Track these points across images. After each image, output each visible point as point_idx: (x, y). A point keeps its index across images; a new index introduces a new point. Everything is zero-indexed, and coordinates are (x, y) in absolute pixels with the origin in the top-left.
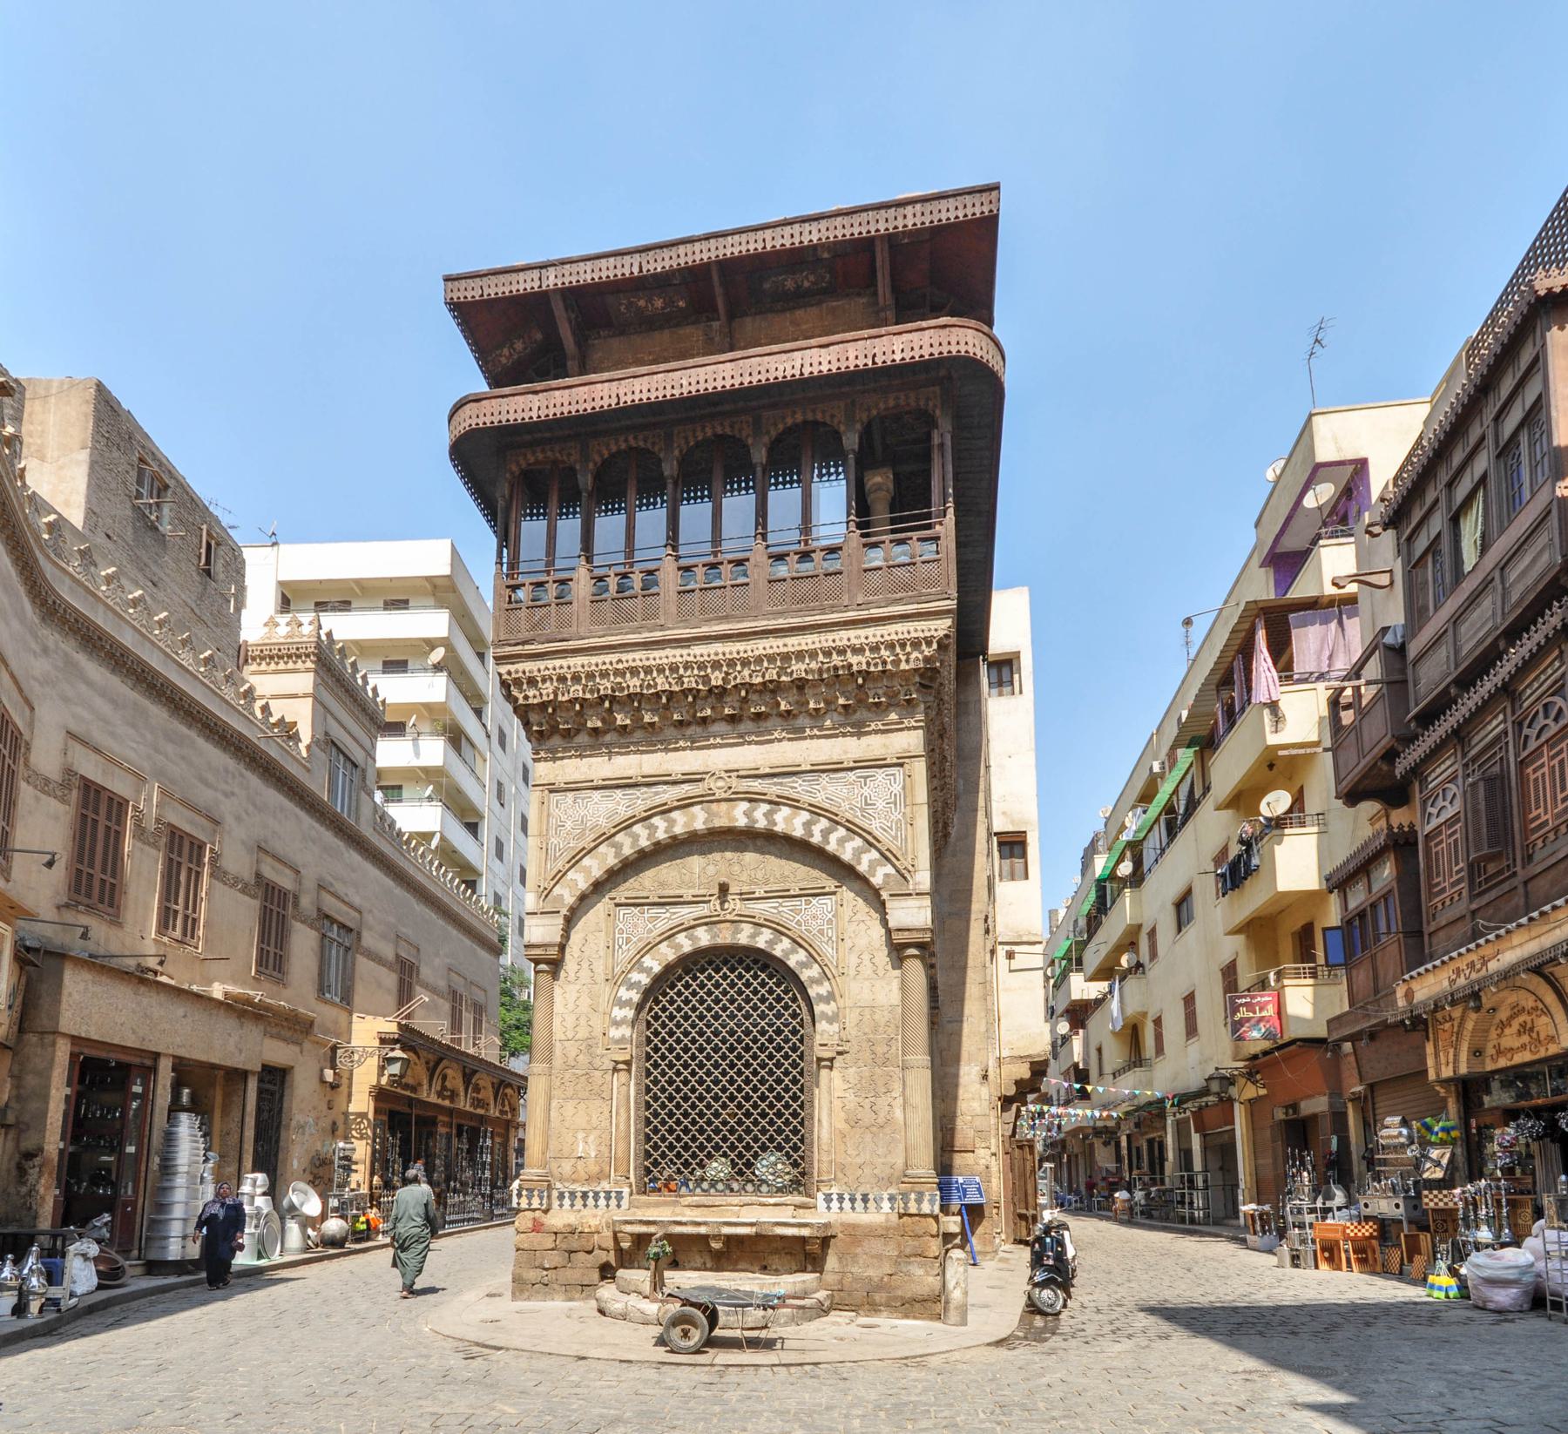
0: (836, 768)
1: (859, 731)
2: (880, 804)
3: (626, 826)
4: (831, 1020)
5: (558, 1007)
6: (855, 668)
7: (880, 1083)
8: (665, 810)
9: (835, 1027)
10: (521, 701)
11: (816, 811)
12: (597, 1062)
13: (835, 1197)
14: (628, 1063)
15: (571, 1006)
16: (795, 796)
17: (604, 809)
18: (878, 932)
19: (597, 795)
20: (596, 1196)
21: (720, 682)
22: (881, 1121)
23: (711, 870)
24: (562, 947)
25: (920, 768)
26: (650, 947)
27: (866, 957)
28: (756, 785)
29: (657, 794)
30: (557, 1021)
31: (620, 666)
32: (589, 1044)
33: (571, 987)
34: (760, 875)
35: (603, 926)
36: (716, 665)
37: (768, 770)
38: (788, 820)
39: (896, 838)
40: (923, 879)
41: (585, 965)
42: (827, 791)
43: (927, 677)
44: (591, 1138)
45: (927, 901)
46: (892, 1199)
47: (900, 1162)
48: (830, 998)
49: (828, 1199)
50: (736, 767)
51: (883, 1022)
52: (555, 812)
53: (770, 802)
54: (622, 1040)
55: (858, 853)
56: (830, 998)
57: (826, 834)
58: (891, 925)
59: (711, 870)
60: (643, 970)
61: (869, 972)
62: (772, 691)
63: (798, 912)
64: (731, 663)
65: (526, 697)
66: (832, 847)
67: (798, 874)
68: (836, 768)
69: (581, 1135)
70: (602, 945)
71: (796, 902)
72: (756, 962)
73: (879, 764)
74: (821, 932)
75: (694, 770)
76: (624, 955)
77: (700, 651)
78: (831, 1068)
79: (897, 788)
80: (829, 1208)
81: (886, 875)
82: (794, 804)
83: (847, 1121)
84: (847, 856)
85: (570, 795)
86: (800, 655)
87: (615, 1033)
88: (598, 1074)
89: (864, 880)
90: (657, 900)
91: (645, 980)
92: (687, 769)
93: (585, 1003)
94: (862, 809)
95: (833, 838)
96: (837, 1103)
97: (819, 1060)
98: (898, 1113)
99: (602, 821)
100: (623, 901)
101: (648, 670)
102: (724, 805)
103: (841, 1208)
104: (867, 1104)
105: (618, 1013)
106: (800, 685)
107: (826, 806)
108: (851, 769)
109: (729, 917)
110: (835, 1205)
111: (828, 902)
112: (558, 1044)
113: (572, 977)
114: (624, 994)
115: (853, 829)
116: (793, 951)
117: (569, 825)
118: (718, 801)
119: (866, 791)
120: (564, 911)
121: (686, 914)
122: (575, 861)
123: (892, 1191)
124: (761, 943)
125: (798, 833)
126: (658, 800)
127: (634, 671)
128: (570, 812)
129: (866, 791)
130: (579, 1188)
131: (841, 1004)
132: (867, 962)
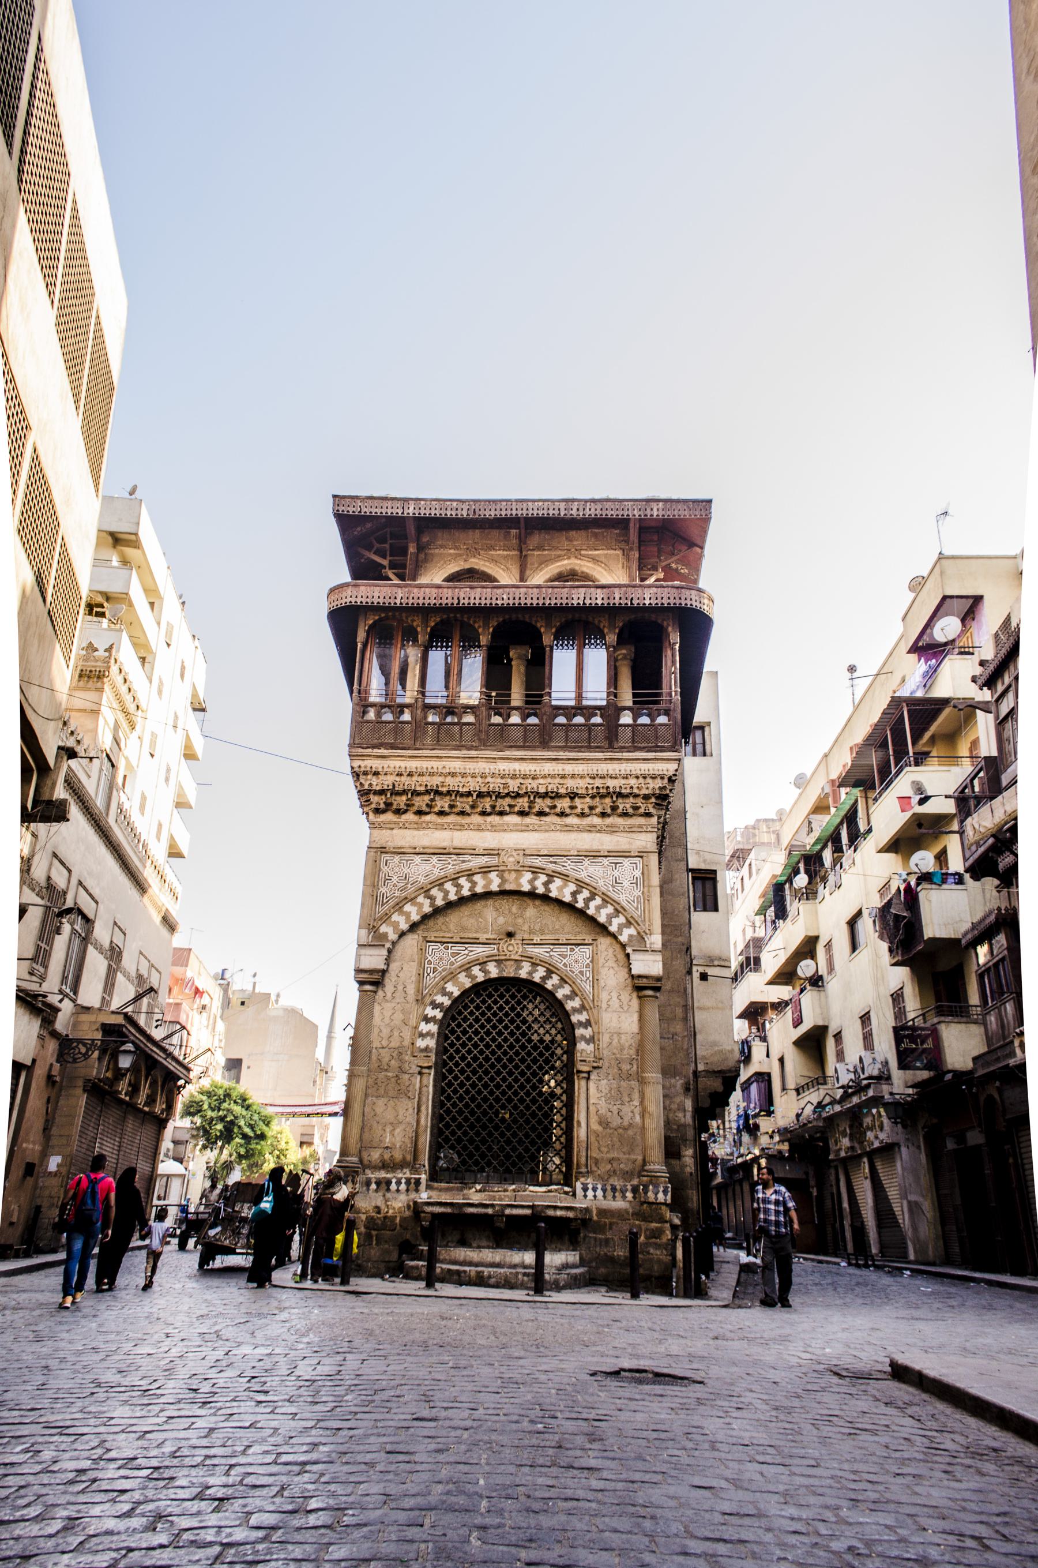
0: (594, 855)
1: (612, 830)
2: (626, 884)
3: (439, 883)
4: (591, 1040)
6: (611, 790)
7: (625, 1095)
8: (470, 875)
9: (590, 1048)
10: (366, 787)
11: (581, 885)
12: (406, 1066)
13: (590, 1186)
14: (429, 1068)
15: (387, 1020)
16: (566, 872)
17: (422, 870)
18: (623, 974)
19: (417, 859)
20: (399, 1183)
21: (516, 790)
22: (626, 1123)
23: (501, 920)
24: (384, 972)
25: (654, 859)
26: (452, 976)
27: (614, 995)
28: (538, 862)
29: (464, 862)
30: (376, 1031)
31: (444, 771)
33: (388, 1005)
34: (537, 927)
35: (416, 957)
36: (514, 777)
37: (546, 853)
38: (560, 889)
39: (637, 909)
40: (656, 940)
41: (400, 988)
42: (588, 871)
43: (662, 799)
44: (398, 1130)
45: (659, 957)
46: (635, 1190)
47: (640, 1158)
48: (587, 1024)
49: (585, 1189)
50: (523, 847)
51: (627, 1045)
52: (385, 869)
53: (547, 875)
54: (427, 1049)
55: (610, 917)
56: (587, 1024)
57: (587, 901)
58: (634, 972)
59: (501, 920)
60: (444, 993)
61: (617, 1006)
62: (552, 798)
63: (565, 957)
64: (525, 777)
65: (370, 785)
66: (591, 912)
67: (565, 925)
68: (594, 855)
69: (388, 1130)
70: (414, 972)
71: (563, 949)
72: (530, 991)
73: (625, 854)
74: (581, 972)
75: (492, 847)
76: (431, 980)
78: (588, 1079)
79: (638, 873)
80: (585, 1196)
81: (631, 936)
82: (565, 877)
83: (600, 1123)
84: (602, 919)
85: (397, 858)
86: (573, 776)
87: (421, 1043)
88: (407, 1076)
89: (614, 936)
90: (458, 940)
91: (447, 1002)
92: (487, 845)
93: (399, 1017)
94: (613, 886)
95: (592, 905)
96: (592, 1108)
97: (579, 1072)
98: (638, 1118)
99: (422, 880)
100: (433, 939)
101: (464, 775)
102: (513, 875)
103: (595, 1196)
104: (615, 1109)
105: (424, 1027)
106: (573, 796)
107: (587, 881)
108: (606, 856)
109: (512, 957)
110: (590, 1193)
111: (587, 951)
112: (374, 1050)
113: (389, 994)
114: (430, 1012)
115: (606, 900)
116: (561, 986)
117: (395, 879)
118: (510, 871)
119: (616, 873)
120: (388, 945)
121: (480, 951)
122: (399, 907)
123: (635, 1182)
124: (537, 978)
125: (567, 899)
126: (465, 866)
127: (453, 775)
128: (397, 869)
129: (616, 873)
130: (383, 1174)
131: (596, 1030)
132: (615, 998)
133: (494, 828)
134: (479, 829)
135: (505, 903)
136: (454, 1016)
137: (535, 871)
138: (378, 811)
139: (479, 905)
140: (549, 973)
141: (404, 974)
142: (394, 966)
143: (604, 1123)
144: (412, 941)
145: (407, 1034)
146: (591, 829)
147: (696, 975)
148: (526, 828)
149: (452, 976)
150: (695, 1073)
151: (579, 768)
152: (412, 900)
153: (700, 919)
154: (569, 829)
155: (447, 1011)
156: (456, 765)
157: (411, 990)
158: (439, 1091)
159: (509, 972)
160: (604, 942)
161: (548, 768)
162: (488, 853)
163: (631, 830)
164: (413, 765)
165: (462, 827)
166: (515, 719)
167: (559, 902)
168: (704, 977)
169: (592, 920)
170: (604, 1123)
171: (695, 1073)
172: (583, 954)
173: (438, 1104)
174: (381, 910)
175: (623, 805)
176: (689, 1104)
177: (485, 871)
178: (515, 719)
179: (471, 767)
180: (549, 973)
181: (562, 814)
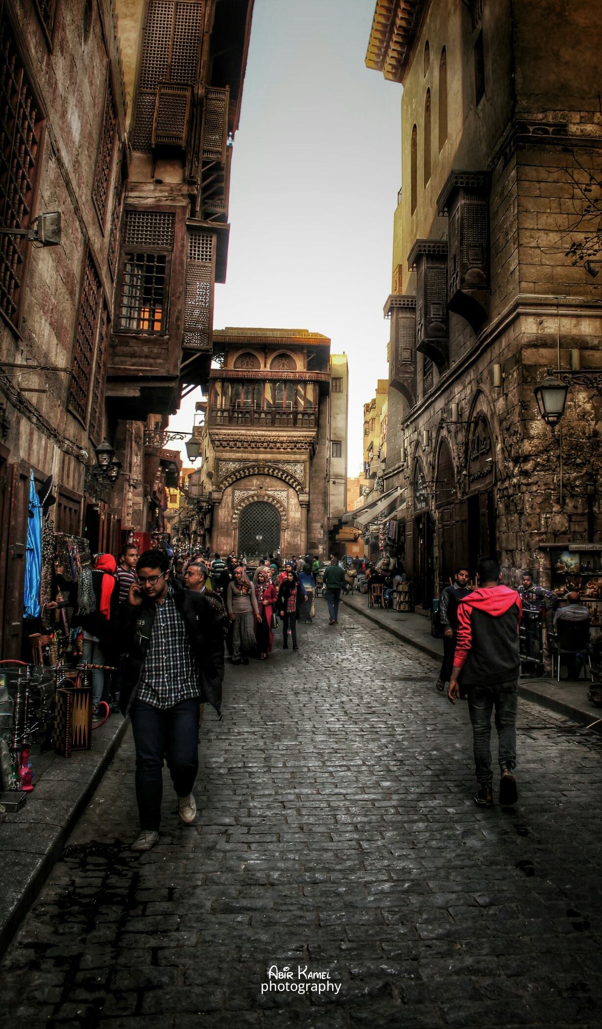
0: (288, 462)
1: (295, 453)
3: (238, 471)
4: (286, 520)
5: (220, 514)
11: (284, 472)
17: (232, 466)
25: (308, 464)
32: (227, 523)
40: (307, 489)
42: (288, 467)
60: (240, 505)
68: (288, 462)
76: (236, 501)
77: (259, 433)
82: (279, 470)
106: (282, 443)
111: (286, 493)
115: (292, 477)
121: (252, 493)
133: (256, 453)
134: (251, 453)
135: (259, 477)
136: (244, 513)
137: (270, 467)
138: (218, 447)
139: (251, 478)
140: (274, 500)
141: (228, 499)
142: (225, 497)
143: (289, 543)
144: (229, 490)
145: (229, 518)
146: (288, 453)
147: (331, 481)
148: (266, 453)
149: (243, 500)
150: (329, 518)
151: (284, 434)
152: (230, 477)
153: (334, 460)
154: (280, 453)
155: (241, 511)
156: (243, 432)
157: (230, 505)
158: (240, 535)
159: (261, 500)
160: (291, 490)
161: (274, 433)
162: (254, 461)
163: (301, 454)
164: (229, 431)
165: (245, 452)
166: (263, 415)
167: (276, 477)
168: (334, 483)
169: (287, 483)
170: (289, 543)
171: (329, 518)
172: (284, 494)
173: (240, 538)
174: (220, 480)
175: (299, 445)
176: (322, 532)
177: (253, 467)
178: (263, 415)
179: (248, 433)
180: (274, 500)
181: (278, 448)
